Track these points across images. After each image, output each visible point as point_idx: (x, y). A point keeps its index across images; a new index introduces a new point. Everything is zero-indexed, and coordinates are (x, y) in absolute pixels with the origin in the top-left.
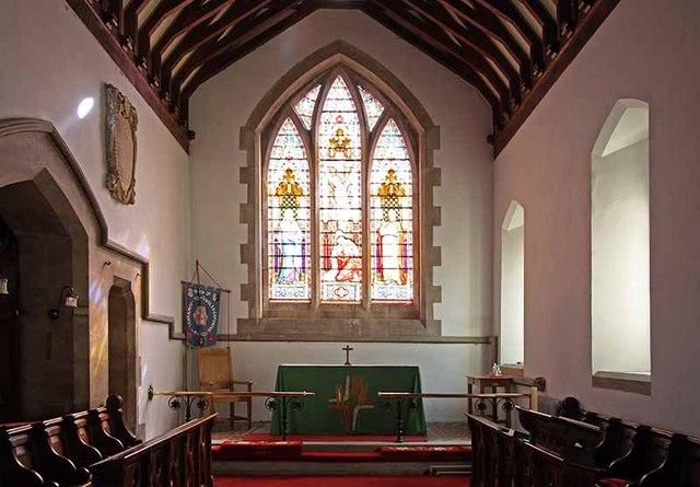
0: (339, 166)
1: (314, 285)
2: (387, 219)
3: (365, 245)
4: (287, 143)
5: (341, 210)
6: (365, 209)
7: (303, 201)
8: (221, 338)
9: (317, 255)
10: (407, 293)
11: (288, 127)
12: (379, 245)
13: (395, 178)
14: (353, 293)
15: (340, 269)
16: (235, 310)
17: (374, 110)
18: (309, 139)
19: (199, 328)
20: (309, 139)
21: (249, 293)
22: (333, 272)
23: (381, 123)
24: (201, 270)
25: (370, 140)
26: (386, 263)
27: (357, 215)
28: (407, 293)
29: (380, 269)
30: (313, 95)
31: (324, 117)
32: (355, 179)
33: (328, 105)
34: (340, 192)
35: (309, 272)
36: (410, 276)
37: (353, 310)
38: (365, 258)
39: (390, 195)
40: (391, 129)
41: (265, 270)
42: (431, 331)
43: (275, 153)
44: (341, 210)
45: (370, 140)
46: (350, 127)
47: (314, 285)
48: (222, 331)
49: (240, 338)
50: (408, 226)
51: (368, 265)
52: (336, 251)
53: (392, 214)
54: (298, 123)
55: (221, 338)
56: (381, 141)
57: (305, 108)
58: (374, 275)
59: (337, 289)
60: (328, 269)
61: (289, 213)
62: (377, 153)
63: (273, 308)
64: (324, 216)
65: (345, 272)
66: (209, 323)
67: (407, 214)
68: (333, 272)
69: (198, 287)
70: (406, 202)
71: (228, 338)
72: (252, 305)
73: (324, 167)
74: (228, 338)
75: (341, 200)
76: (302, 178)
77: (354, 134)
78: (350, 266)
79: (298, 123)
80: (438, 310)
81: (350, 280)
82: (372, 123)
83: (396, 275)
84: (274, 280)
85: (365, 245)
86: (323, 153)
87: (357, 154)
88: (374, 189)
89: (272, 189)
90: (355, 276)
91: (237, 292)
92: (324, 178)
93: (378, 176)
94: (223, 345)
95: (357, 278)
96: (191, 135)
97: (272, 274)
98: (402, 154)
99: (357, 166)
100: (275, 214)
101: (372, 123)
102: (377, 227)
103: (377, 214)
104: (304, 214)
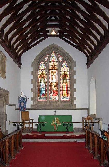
0: (53, 71)
2: (64, 82)
5: (54, 81)
6: (59, 80)
11: (43, 63)
12: (62, 88)
13: (66, 73)
15: (53, 93)
22: (52, 94)
23: (63, 61)
25: (60, 65)
26: (64, 92)
29: (62, 93)
32: (57, 73)
33: (51, 58)
34: (54, 76)
39: (65, 76)
40: (65, 63)
44: (54, 81)
46: (56, 62)
53: (65, 81)
56: (63, 65)
60: (51, 93)
68: (52, 94)
75: (54, 79)
77: (56, 63)
78: (55, 93)
82: (60, 62)
101: (60, 62)
102: (62, 84)
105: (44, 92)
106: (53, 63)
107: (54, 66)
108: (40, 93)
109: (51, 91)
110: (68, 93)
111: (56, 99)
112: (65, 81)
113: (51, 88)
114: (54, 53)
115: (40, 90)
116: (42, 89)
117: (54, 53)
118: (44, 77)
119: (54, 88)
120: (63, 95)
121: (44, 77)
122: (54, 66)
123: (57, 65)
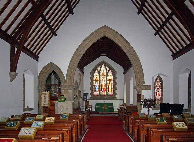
0: (103, 76)
1: (100, 93)
2: (110, 84)
3: (107, 87)
4: (96, 74)
5: (104, 83)
6: (107, 82)
7: (98, 81)
9: (100, 88)
10: (112, 93)
11: (96, 71)
12: (108, 87)
14: (105, 93)
15: (103, 90)
16: (89, 96)
17: (108, 69)
18: (99, 73)
20: (99, 73)
22: (102, 91)
25: (107, 73)
26: (109, 89)
27: (106, 83)
28: (112, 93)
29: (109, 90)
30: (100, 67)
31: (101, 70)
32: (105, 78)
34: (103, 80)
37: (105, 95)
38: (107, 89)
39: (110, 80)
40: (110, 71)
42: (115, 99)
43: (95, 75)
44: (104, 83)
45: (107, 73)
47: (100, 93)
49: (89, 100)
50: (112, 84)
51: (107, 90)
52: (103, 88)
53: (110, 83)
54: (98, 71)
56: (109, 73)
57: (99, 69)
59: (102, 93)
60: (101, 90)
61: (96, 83)
62: (108, 75)
64: (101, 83)
67: (112, 83)
68: (102, 91)
70: (112, 81)
71: (89, 100)
73: (101, 76)
74: (89, 100)
76: (98, 78)
77: (105, 72)
79: (98, 71)
80: (116, 96)
83: (111, 91)
85: (107, 87)
86: (101, 75)
87: (106, 75)
88: (108, 80)
89: (94, 80)
91: (90, 94)
92: (101, 78)
93: (108, 78)
96: (84, 73)
98: (112, 75)
99: (106, 76)
100: (94, 83)
103: (108, 83)
104: (98, 83)
105: (97, 90)
106: (103, 72)
107: (103, 74)
108: (95, 90)
109: (101, 89)
110: (112, 90)
112: (110, 83)
113: (102, 87)
114: (103, 65)
115: (95, 89)
116: (96, 88)
117: (103, 65)
118: (97, 80)
119: (104, 87)
120: (109, 92)
121: (97, 80)
122: (103, 74)
123: (105, 73)
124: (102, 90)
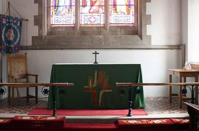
8: (22, 48)
10: (130, 20)
14: (98, 20)
15: (92, 6)
19: (9, 42)
21: (38, 21)
24: (10, 5)
29: (115, 5)
35: (74, 8)
36: (132, 9)
37: (100, 30)
41: (49, 8)
42: (145, 41)
48: (24, 44)
49: (34, 47)
55: (22, 48)
58: (111, 9)
60: (84, 6)
63: (53, 30)
65: (94, 8)
66: (15, 39)
68: (88, 8)
69: (9, 17)
71: (27, 48)
72: (41, 28)
74: (27, 48)
78: (97, 4)
81: (98, 12)
83: (124, 9)
84: (54, 13)
90: (100, 10)
91: (32, 20)
94: (22, 52)
95: (102, 11)
97: (52, 10)
111: (99, 22)
124: (89, 4)
